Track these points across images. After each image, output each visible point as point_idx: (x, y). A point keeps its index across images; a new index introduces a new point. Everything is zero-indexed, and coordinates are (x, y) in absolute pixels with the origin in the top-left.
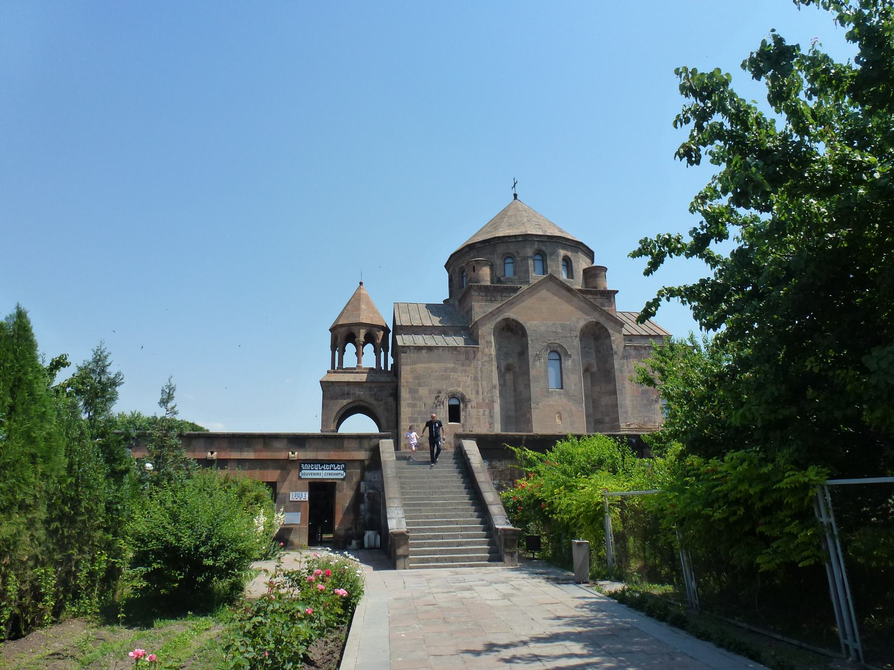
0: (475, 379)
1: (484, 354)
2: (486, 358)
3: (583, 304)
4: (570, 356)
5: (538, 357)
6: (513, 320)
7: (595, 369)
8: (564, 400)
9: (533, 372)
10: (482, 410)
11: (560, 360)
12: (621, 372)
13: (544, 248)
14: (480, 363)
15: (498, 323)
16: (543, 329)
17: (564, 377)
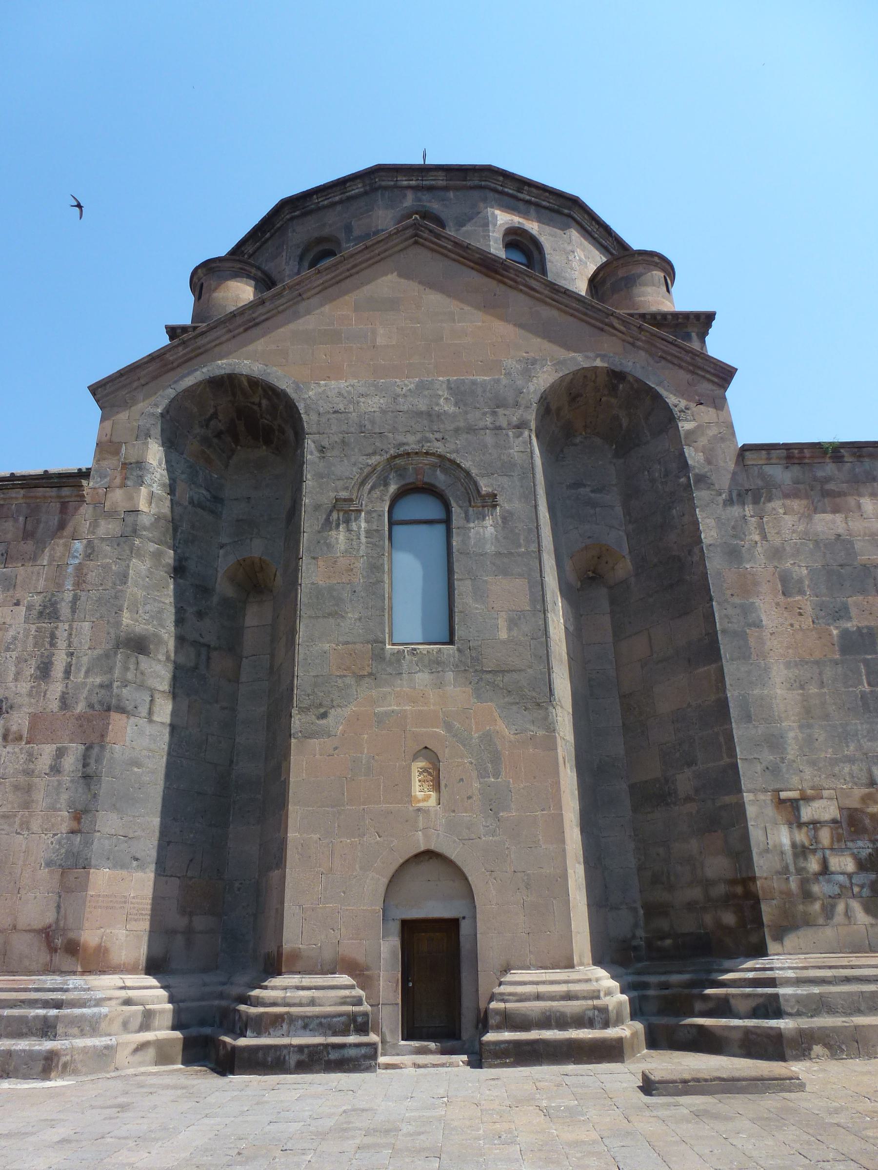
0: (49, 612)
1: (103, 512)
2: (108, 528)
3: (547, 313)
4: (490, 501)
5: (343, 510)
6: (254, 383)
7: (624, 568)
8: (457, 693)
9: (312, 575)
10: (47, 751)
11: (447, 521)
12: (734, 554)
13: (435, 206)
14: (78, 546)
15: (189, 392)
16: (374, 404)
17: (463, 587)
